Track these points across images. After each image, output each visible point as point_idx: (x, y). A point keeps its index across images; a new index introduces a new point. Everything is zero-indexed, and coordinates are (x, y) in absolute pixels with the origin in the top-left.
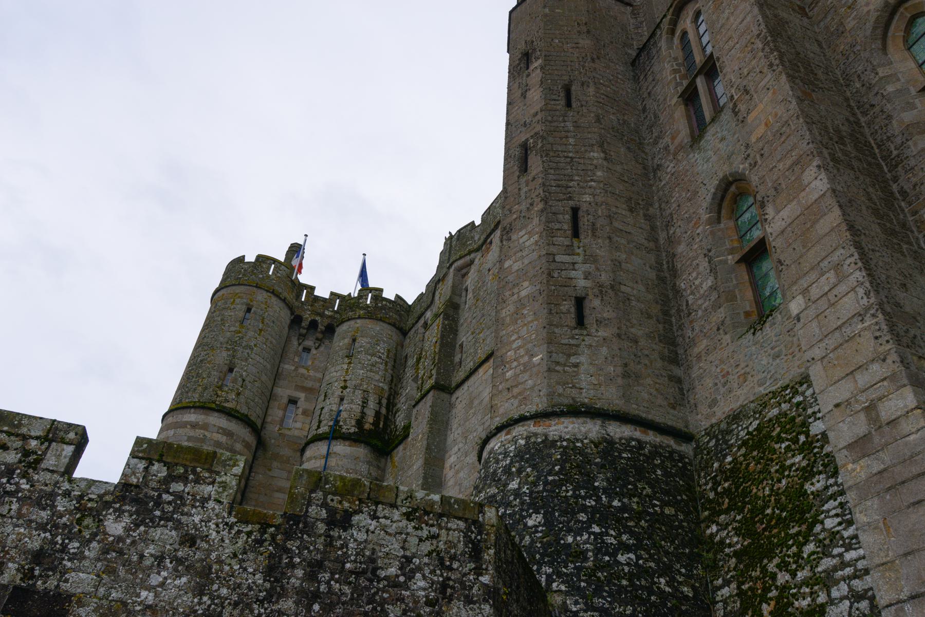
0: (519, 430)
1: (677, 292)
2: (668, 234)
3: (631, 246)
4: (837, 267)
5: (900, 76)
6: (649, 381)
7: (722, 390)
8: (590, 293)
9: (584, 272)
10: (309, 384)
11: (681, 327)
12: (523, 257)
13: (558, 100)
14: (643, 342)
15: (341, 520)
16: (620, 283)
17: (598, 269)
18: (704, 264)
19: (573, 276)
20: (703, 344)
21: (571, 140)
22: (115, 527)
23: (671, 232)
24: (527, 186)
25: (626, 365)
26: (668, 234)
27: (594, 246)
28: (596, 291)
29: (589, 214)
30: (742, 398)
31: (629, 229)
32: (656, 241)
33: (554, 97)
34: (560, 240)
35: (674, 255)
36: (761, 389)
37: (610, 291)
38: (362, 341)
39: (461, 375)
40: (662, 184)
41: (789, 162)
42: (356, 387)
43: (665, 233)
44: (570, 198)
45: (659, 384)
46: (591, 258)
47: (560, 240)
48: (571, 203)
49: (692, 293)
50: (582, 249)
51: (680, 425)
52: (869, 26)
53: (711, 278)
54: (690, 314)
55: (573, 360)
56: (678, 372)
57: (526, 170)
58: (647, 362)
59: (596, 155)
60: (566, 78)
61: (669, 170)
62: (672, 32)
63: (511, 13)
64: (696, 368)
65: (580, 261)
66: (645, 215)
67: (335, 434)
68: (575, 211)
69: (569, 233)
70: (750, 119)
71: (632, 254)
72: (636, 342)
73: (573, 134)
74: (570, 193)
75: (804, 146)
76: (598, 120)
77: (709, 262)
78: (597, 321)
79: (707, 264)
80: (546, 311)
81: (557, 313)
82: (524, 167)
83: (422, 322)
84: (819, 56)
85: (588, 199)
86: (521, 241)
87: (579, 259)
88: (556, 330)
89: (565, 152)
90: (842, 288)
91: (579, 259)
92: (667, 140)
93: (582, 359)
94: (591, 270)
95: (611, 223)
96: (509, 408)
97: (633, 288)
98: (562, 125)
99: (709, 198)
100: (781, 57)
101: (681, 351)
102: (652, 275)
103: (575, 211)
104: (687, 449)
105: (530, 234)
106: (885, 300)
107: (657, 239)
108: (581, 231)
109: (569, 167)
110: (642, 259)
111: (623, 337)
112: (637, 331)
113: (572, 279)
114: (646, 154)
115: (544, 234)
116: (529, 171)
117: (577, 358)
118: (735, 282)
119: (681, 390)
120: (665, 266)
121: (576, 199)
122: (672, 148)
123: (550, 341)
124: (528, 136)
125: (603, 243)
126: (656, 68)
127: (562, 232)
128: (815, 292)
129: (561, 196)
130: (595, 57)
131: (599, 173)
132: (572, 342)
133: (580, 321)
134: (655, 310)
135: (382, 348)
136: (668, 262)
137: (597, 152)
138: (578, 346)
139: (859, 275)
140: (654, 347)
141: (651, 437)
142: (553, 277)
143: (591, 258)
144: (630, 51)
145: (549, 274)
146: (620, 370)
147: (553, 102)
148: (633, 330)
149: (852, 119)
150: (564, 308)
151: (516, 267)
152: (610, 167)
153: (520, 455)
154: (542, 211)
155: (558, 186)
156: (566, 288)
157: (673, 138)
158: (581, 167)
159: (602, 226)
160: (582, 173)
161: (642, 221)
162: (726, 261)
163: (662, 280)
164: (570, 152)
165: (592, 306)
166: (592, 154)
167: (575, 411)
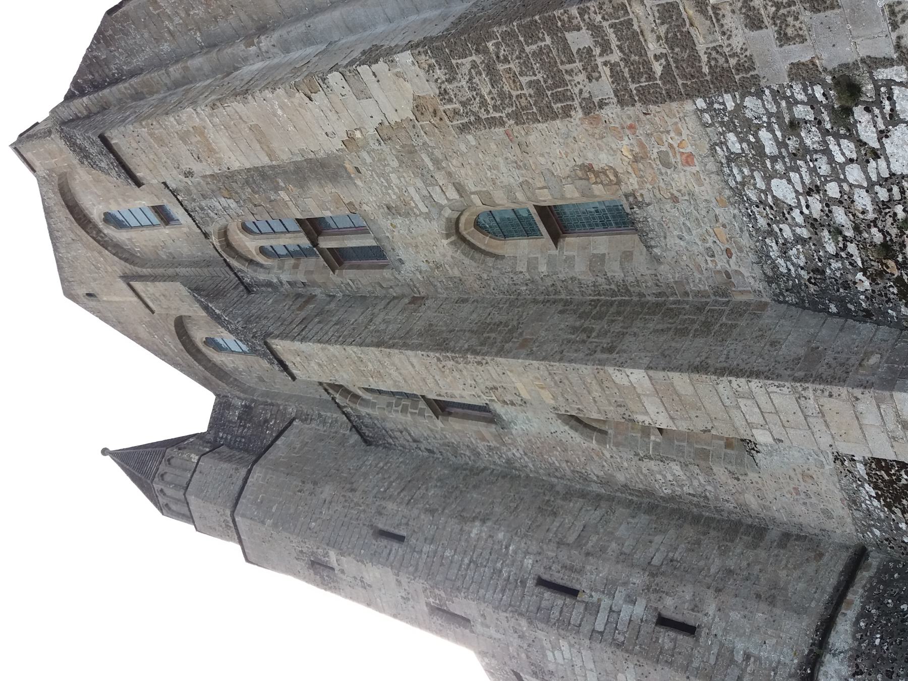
1: (672, 498)
2: (596, 482)
3: (602, 530)
4: (737, 395)
5: (532, 256)
6: (783, 574)
7: (814, 500)
8: (655, 605)
9: (625, 601)
11: (719, 510)
12: (583, 667)
13: (391, 550)
14: (731, 564)
16: (649, 563)
17: (625, 584)
18: (652, 464)
19: (628, 618)
21: (447, 554)
23: (595, 478)
24: (488, 627)
25: (758, 596)
26: (596, 482)
27: (593, 577)
28: (653, 596)
29: (550, 568)
30: (832, 487)
31: (579, 525)
32: (599, 497)
33: (385, 554)
35: (626, 486)
36: (827, 467)
37: (658, 580)
40: (530, 465)
41: (595, 386)
43: (593, 485)
44: (524, 583)
45: (788, 562)
46: (610, 587)
47: (575, 618)
48: (530, 583)
49: (681, 486)
50: (593, 594)
51: (844, 557)
52: (467, 261)
53: (672, 464)
54: (706, 497)
55: (739, 658)
56: (774, 534)
57: (468, 621)
58: (758, 567)
59: (475, 531)
60: (365, 530)
61: (517, 455)
63: (247, 560)
64: (776, 515)
65: (610, 602)
66: (565, 498)
68: (542, 582)
69: (568, 600)
70: (525, 395)
71: (612, 533)
72: (730, 572)
73: (440, 549)
74: (516, 581)
75: (587, 370)
76: (432, 511)
77: (651, 459)
78: (693, 610)
79: (653, 462)
80: (666, 669)
81: (673, 656)
82: (464, 621)
84: (476, 308)
85: (530, 561)
86: (560, 661)
87: (606, 602)
88: (695, 664)
89: (460, 566)
90: (763, 399)
91: (606, 602)
92: (481, 446)
93: (740, 646)
94: (624, 593)
95: (568, 545)
97: (658, 550)
98: (424, 556)
99: (573, 433)
100: (475, 353)
101: (749, 521)
102: (643, 519)
103: (542, 582)
106: (789, 372)
107: (598, 495)
108: (569, 584)
109: (482, 569)
110: (621, 524)
111: (721, 586)
112: (716, 564)
113: (630, 620)
114: (485, 469)
115: (562, 632)
116: (470, 618)
117: (738, 652)
118: (685, 444)
119: (799, 538)
120: (635, 499)
121: (526, 576)
122: (493, 444)
124: (423, 600)
125: (592, 565)
126: (389, 425)
127: (565, 609)
128: (756, 418)
129: (518, 592)
130: (348, 486)
131: (500, 536)
132: (715, 650)
133: (689, 630)
134: (690, 532)
136: (630, 494)
137: (472, 527)
138: (722, 645)
139: (755, 384)
140: (738, 551)
142: (623, 643)
143: (610, 587)
144: (352, 441)
145: (619, 645)
146: (763, 606)
147: (392, 558)
148: (712, 571)
149: (560, 307)
150: (668, 645)
152: (494, 519)
154: (530, 623)
155: (503, 591)
156: (642, 632)
157: (483, 439)
158: (486, 554)
159: (569, 557)
160: (494, 556)
161: (571, 505)
162: (656, 444)
163: (652, 509)
164: (462, 560)
165: (672, 608)
166: (472, 535)
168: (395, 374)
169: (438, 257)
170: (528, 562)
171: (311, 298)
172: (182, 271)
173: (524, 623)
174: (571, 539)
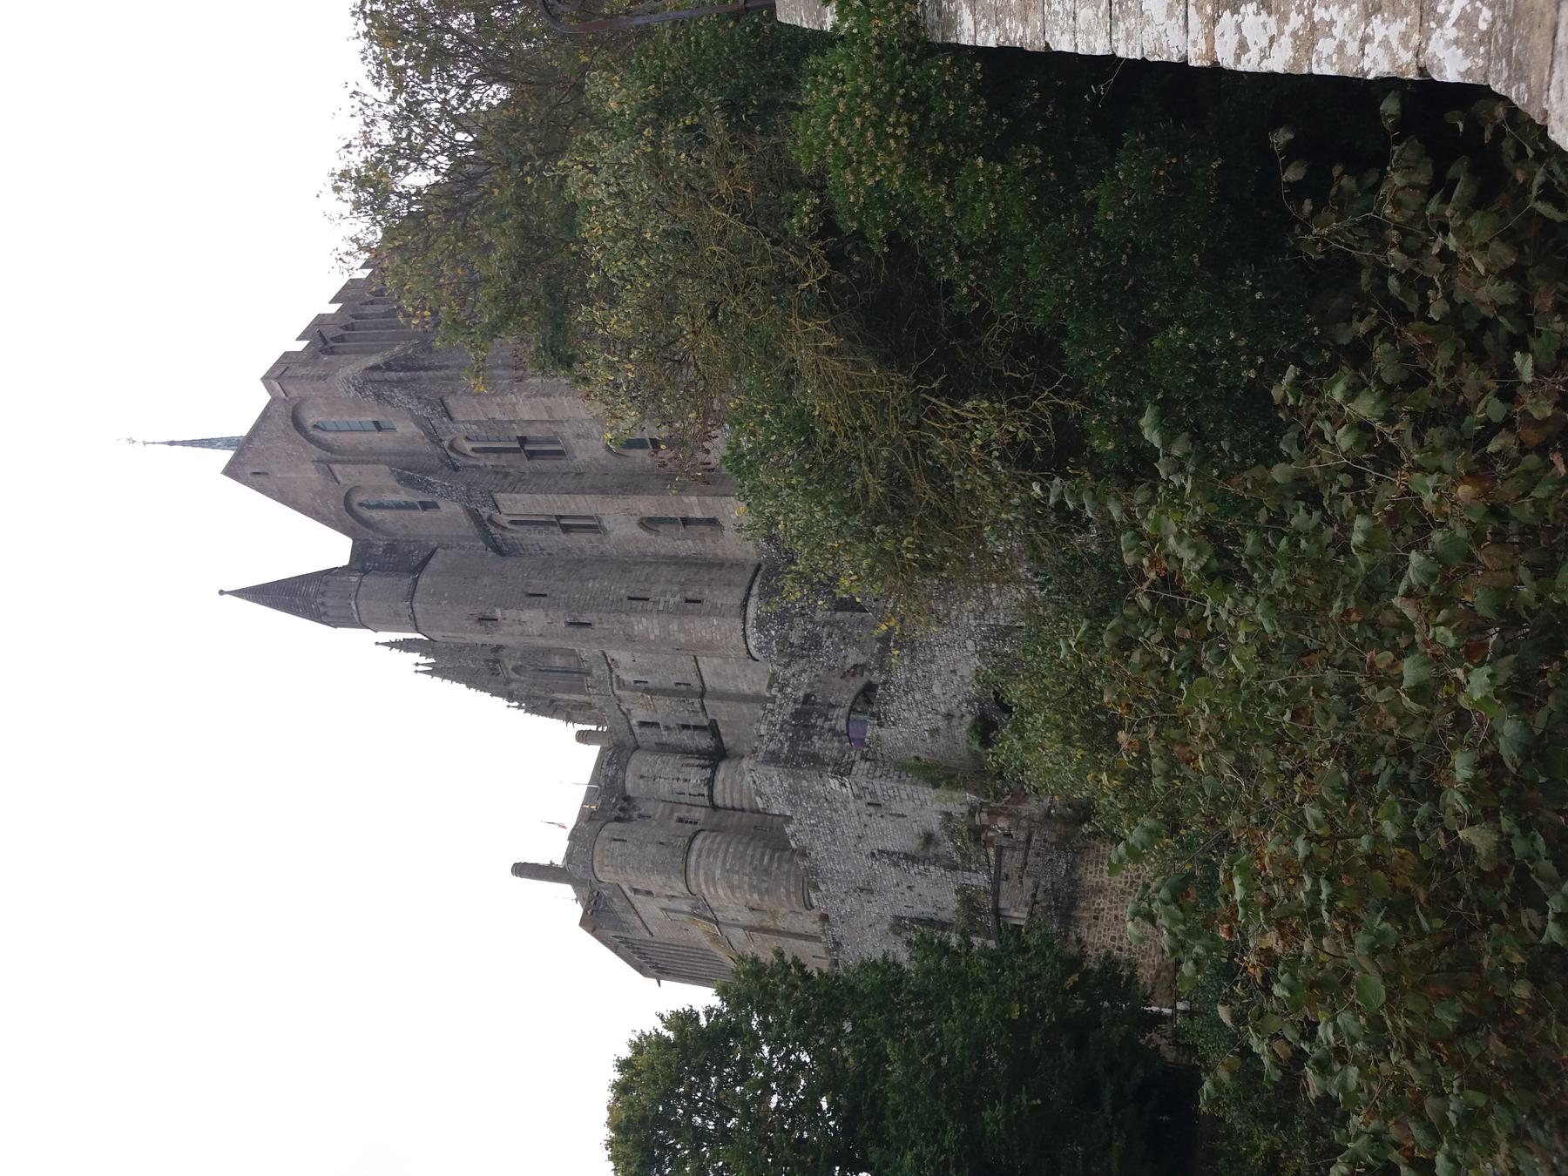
0: (748, 632)
1: (685, 557)
10: (668, 811)
15: (792, 645)
18: (679, 543)
20: (719, 552)
22: (789, 690)
34: (649, 607)
38: (644, 770)
39: (696, 684)
42: (679, 772)
46: (663, 593)
48: (625, 600)
62: (504, 528)
67: (710, 783)
68: (630, 598)
83: (636, 730)
87: (662, 599)
91: (662, 599)
92: (587, 547)
93: (719, 602)
96: (736, 638)
104: (764, 567)
105: (639, 622)
123: (708, 615)
135: (650, 758)
141: (758, 579)
143: (663, 593)
151: (657, 632)
153: (760, 631)
157: (590, 542)
163: (675, 564)
167: (744, 606)
168: (573, 506)
169: (597, 456)
170: (623, 591)
171: (507, 475)
172: (388, 459)
173: (624, 616)
174: (642, 579)
